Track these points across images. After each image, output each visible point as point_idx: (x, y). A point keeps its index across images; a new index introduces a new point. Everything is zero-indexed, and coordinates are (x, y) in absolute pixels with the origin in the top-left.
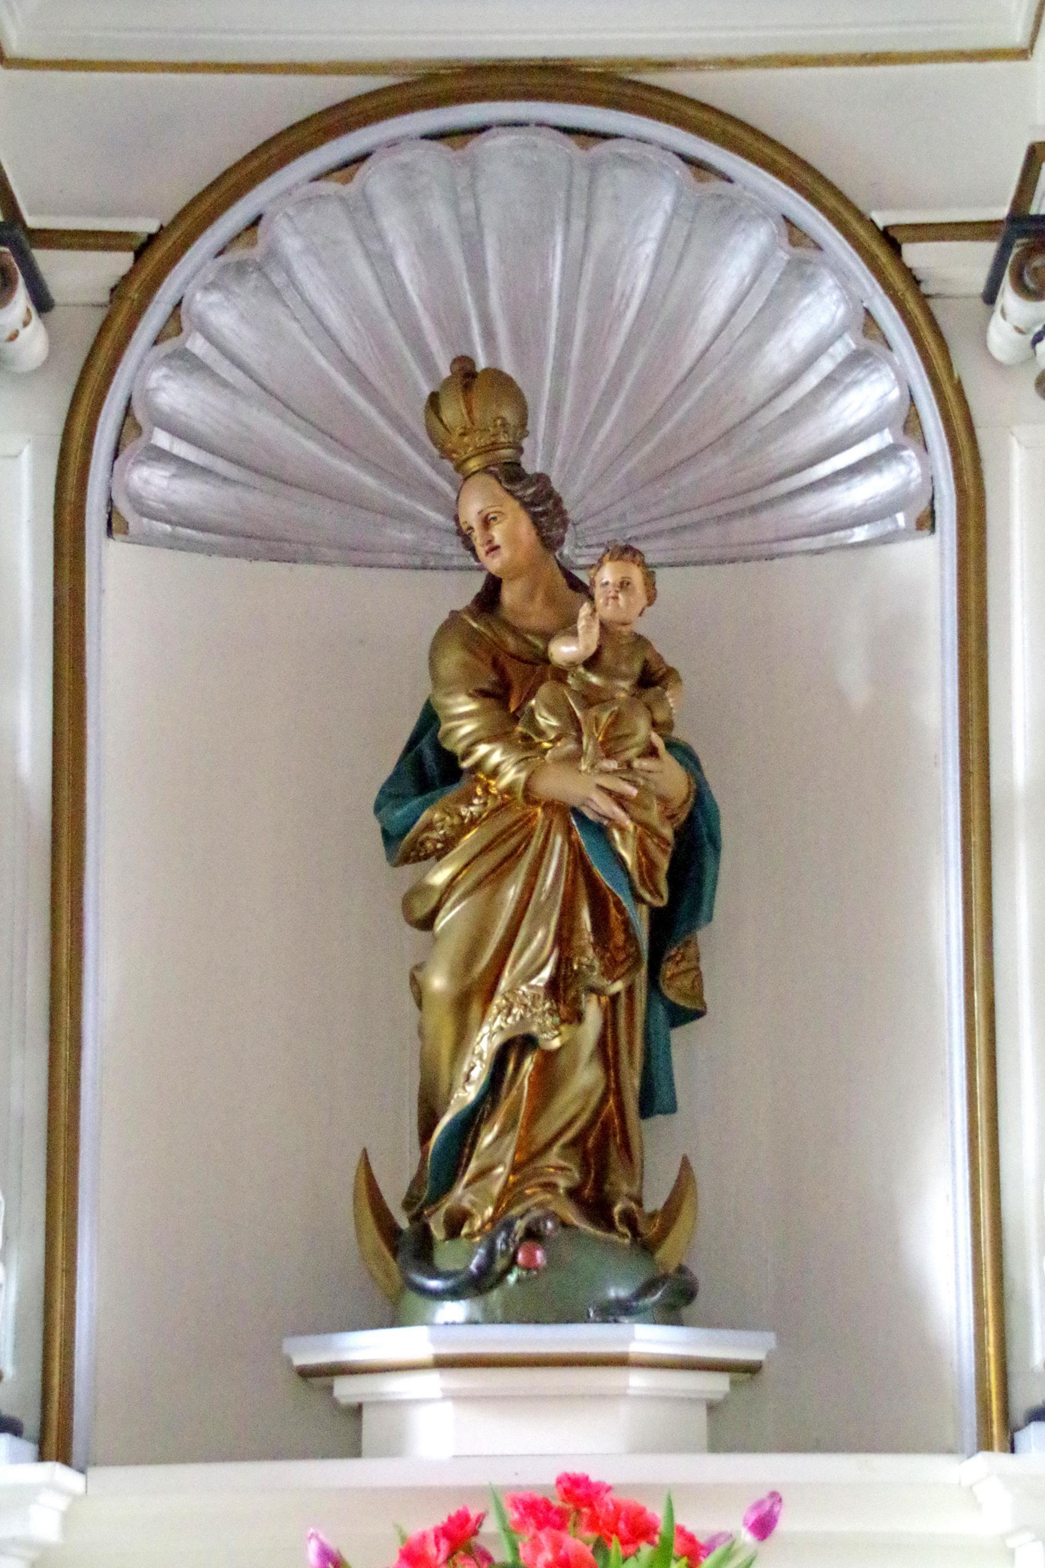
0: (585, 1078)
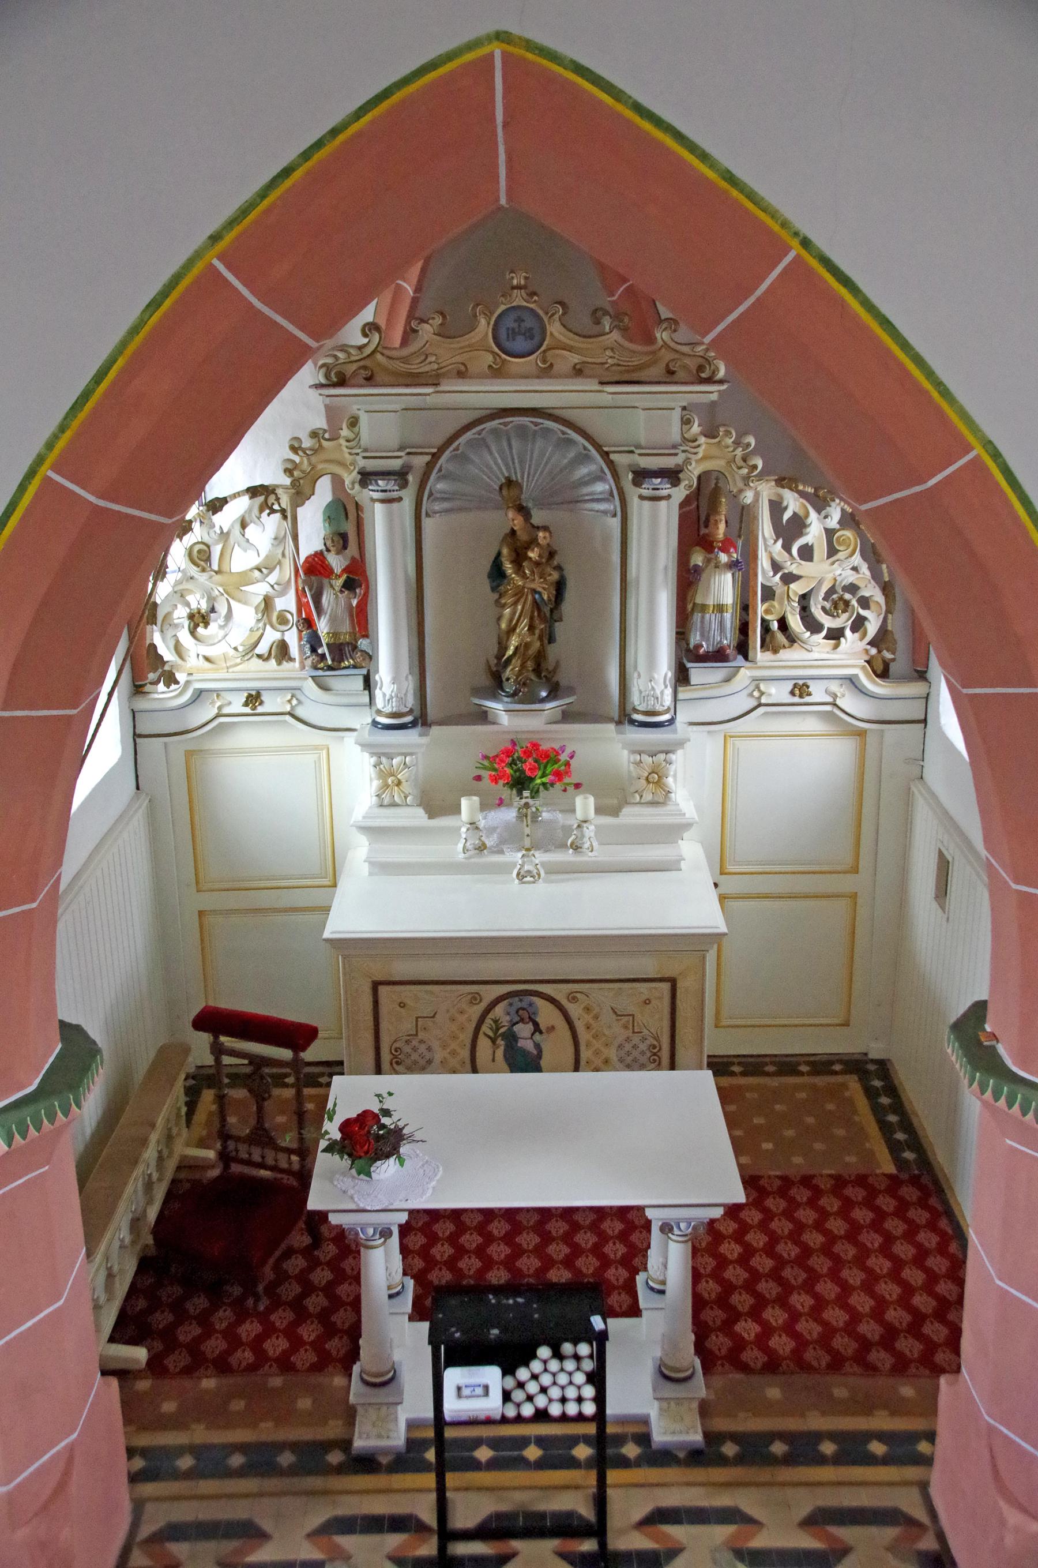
0: (538, 644)
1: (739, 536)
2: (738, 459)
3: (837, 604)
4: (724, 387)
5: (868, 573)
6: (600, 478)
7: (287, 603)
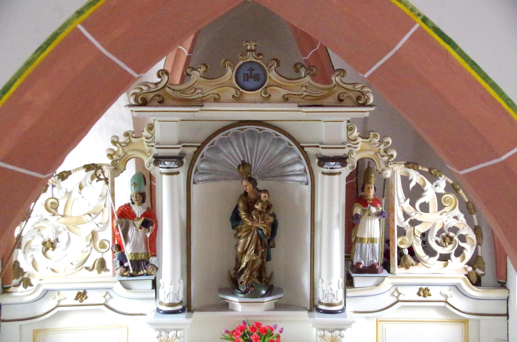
1: (383, 197)
2: (382, 151)
3: (446, 238)
4: (372, 109)
5: (464, 220)
6: (299, 162)
7: (106, 235)
